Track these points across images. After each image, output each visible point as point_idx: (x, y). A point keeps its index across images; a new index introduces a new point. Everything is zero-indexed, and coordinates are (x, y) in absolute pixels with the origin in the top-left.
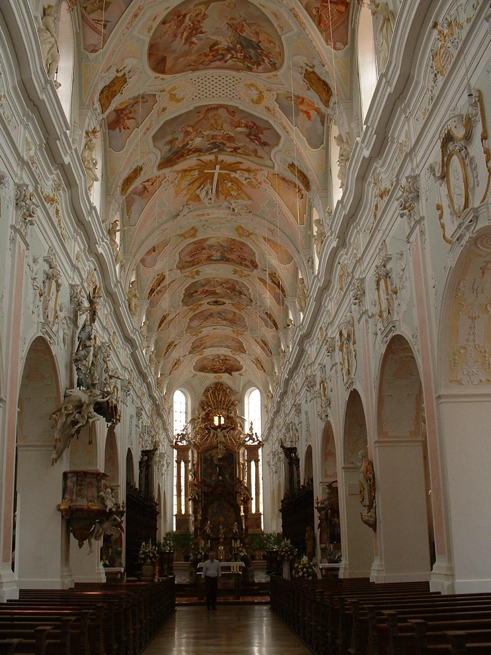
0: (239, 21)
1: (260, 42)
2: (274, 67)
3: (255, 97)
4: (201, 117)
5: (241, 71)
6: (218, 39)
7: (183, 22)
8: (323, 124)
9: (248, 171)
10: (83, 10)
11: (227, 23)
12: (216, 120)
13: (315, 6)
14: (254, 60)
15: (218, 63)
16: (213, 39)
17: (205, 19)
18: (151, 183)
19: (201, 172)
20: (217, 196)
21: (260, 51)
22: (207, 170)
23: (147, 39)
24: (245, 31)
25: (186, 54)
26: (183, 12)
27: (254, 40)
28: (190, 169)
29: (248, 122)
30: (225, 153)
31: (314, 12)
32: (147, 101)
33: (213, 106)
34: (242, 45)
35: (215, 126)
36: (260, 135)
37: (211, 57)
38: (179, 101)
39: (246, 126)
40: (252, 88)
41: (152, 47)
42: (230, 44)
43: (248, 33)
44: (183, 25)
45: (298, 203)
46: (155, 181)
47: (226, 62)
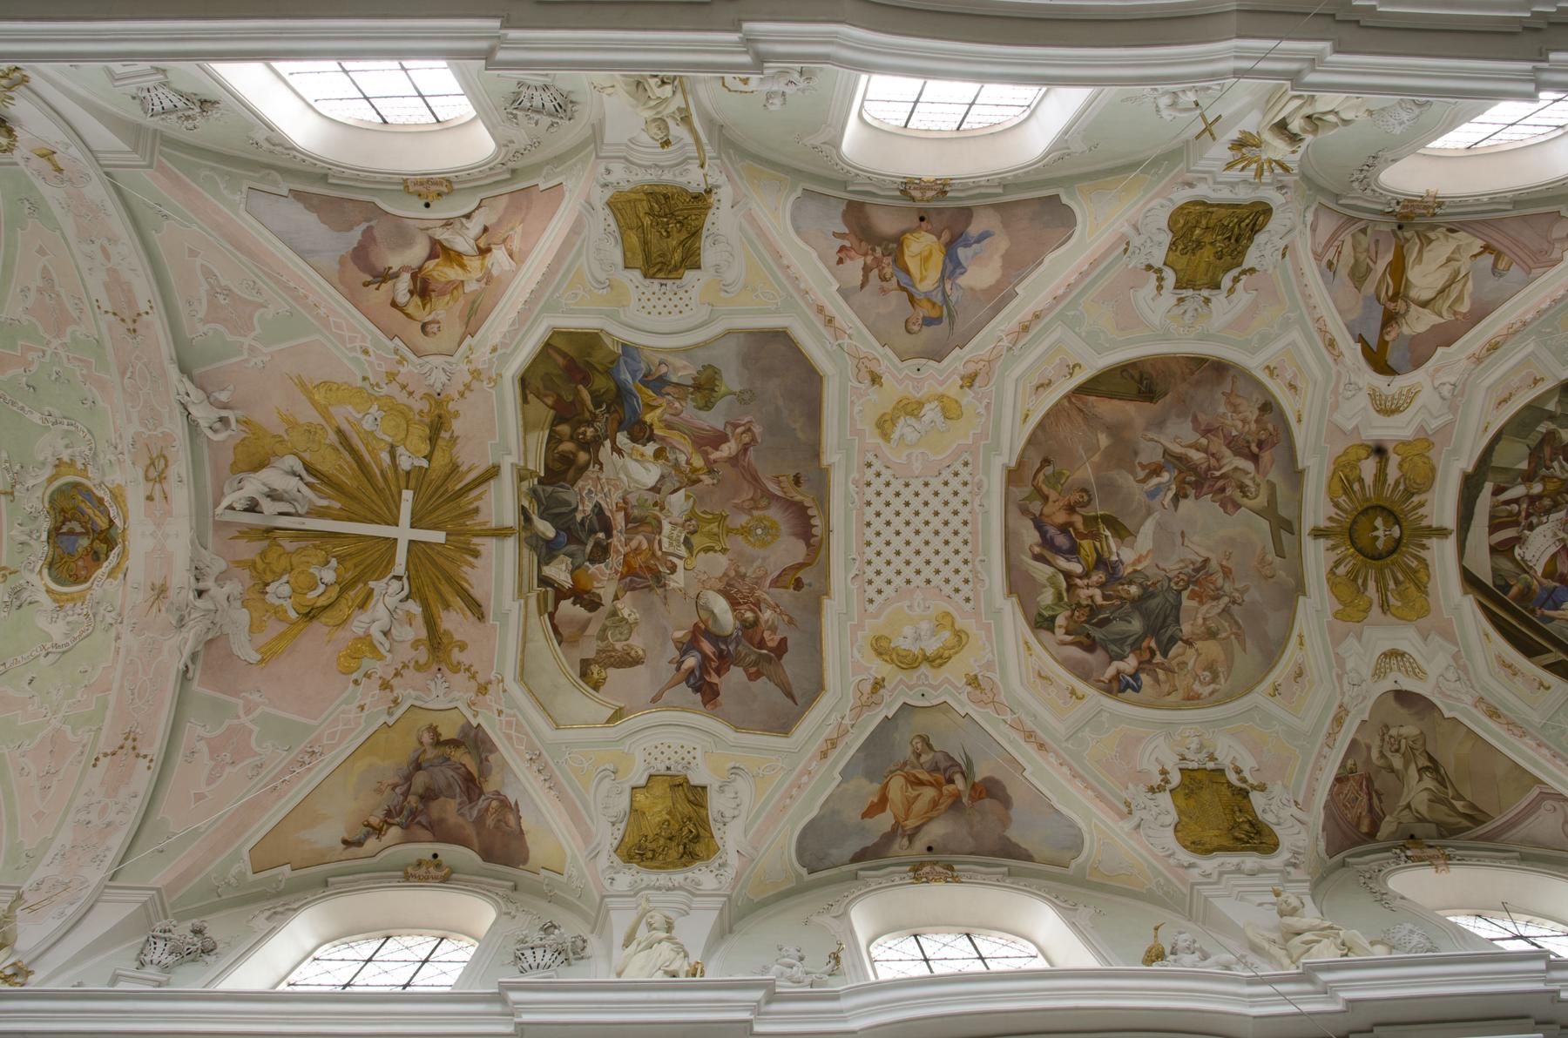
0: (1226, 587)
1: (1189, 643)
2: (1119, 686)
3: (904, 642)
4: (773, 488)
5: (1014, 599)
6: (1140, 537)
7: (1237, 453)
8: (858, 857)
9: (436, 642)
10: (1361, 225)
11: (1207, 561)
12: (746, 531)
13: (1359, 765)
14: (1097, 634)
15: (1031, 536)
16: (1141, 524)
17: (1223, 505)
18: (402, 296)
19: (415, 478)
20: (250, 533)
21: (1153, 644)
22: (415, 501)
23: (1254, 363)
24: (1201, 603)
25: (1122, 452)
26: (1266, 456)
27: (1186, 628)
28: (441, 443)
29: (773, 629)
30: (531, 559)
31: (1350, 763)
32: (908, 331)
33: (813, 522)
34: (1147, 594)
35: (714, 527)
36: (736, 675)
37: (1061, 518)
38: (884, 426)
39: (749, 628)
40: (946, 635)
41: (1219, 369)
42: (1130, 570)
43: (1194, 615)
44: (1228, 453)
45: (328, 834)
46: (407, 315)
47: (1039, 558)
